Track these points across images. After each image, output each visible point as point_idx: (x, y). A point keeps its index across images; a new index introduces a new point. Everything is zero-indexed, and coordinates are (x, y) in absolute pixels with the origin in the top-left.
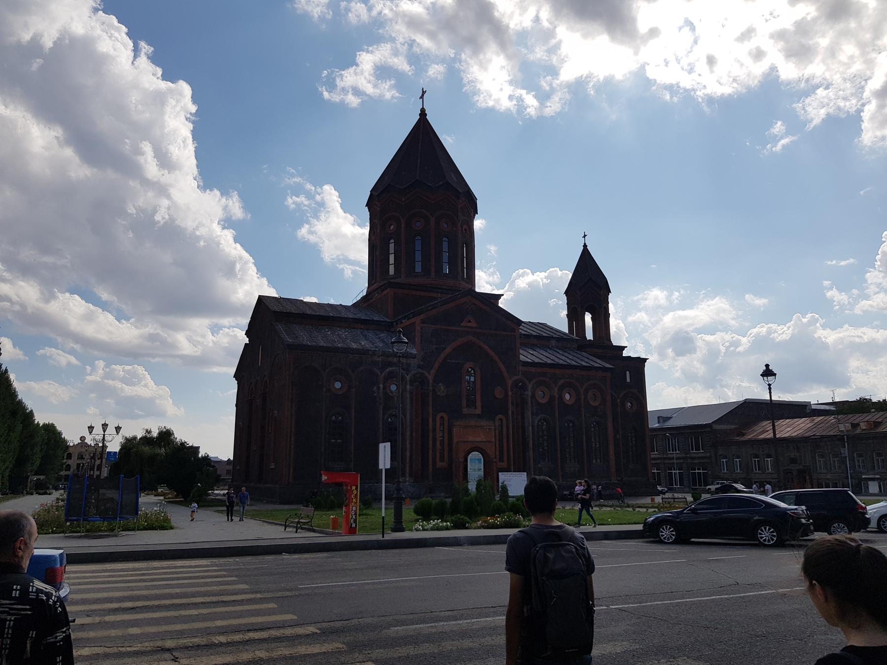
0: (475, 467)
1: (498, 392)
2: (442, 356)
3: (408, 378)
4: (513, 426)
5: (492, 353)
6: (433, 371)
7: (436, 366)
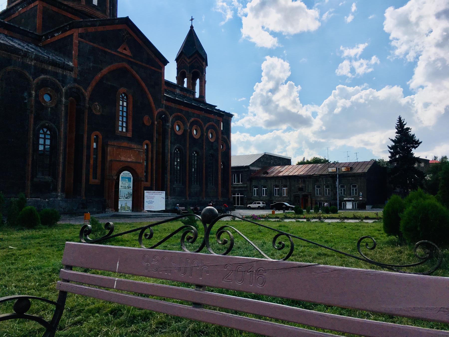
0: (126, 183)
1: (146, 120)
5: (143, 84)
6: (90, 89)
7: (93, 83)
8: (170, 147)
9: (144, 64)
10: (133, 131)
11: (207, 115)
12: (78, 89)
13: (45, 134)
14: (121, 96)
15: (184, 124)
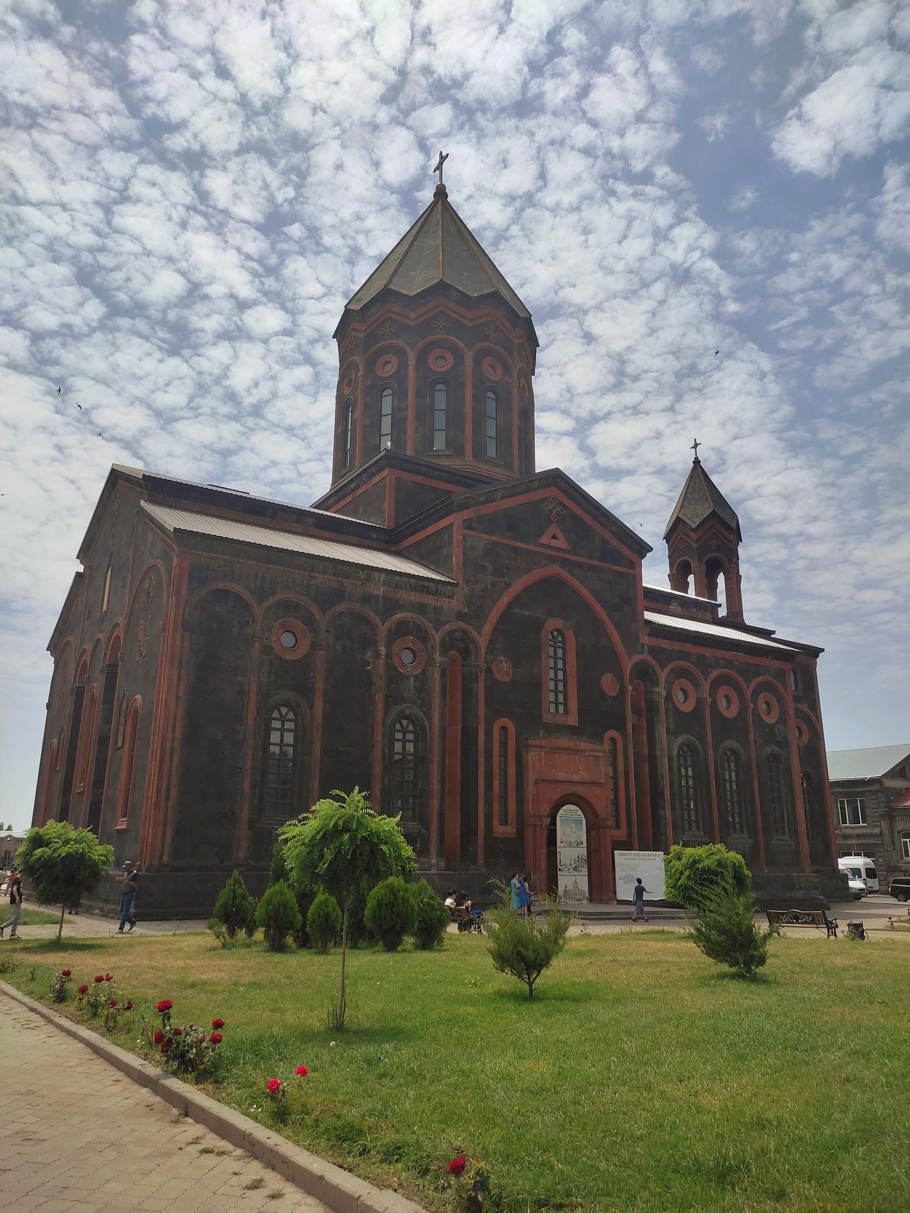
1: (608, 684)
2: (505, 599)
3: (438, 637)
4: (636, 755)
5: (598, 607)
6: (487, 629)
7: (494, 616)
8: (668, 745)
9: (596, 563)
11: (750, 659)
12: (463, 631)
13: (404, 731)
14: (550, 637)
15: (696, 684)
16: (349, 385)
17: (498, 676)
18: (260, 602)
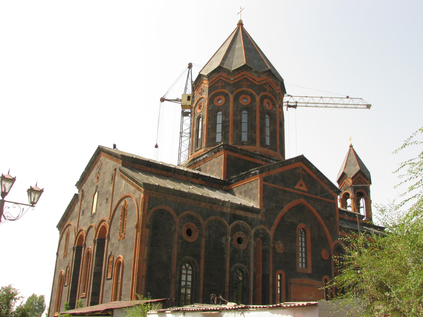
1: (324, 254)
2: (281, 214)
3: (253, 232)
5: (319, 218)
6: (273, 228)
10: (313, 267)
12: (263, 229)
16: (200, 108)
17: (278, 250)
18: (178, 215)
